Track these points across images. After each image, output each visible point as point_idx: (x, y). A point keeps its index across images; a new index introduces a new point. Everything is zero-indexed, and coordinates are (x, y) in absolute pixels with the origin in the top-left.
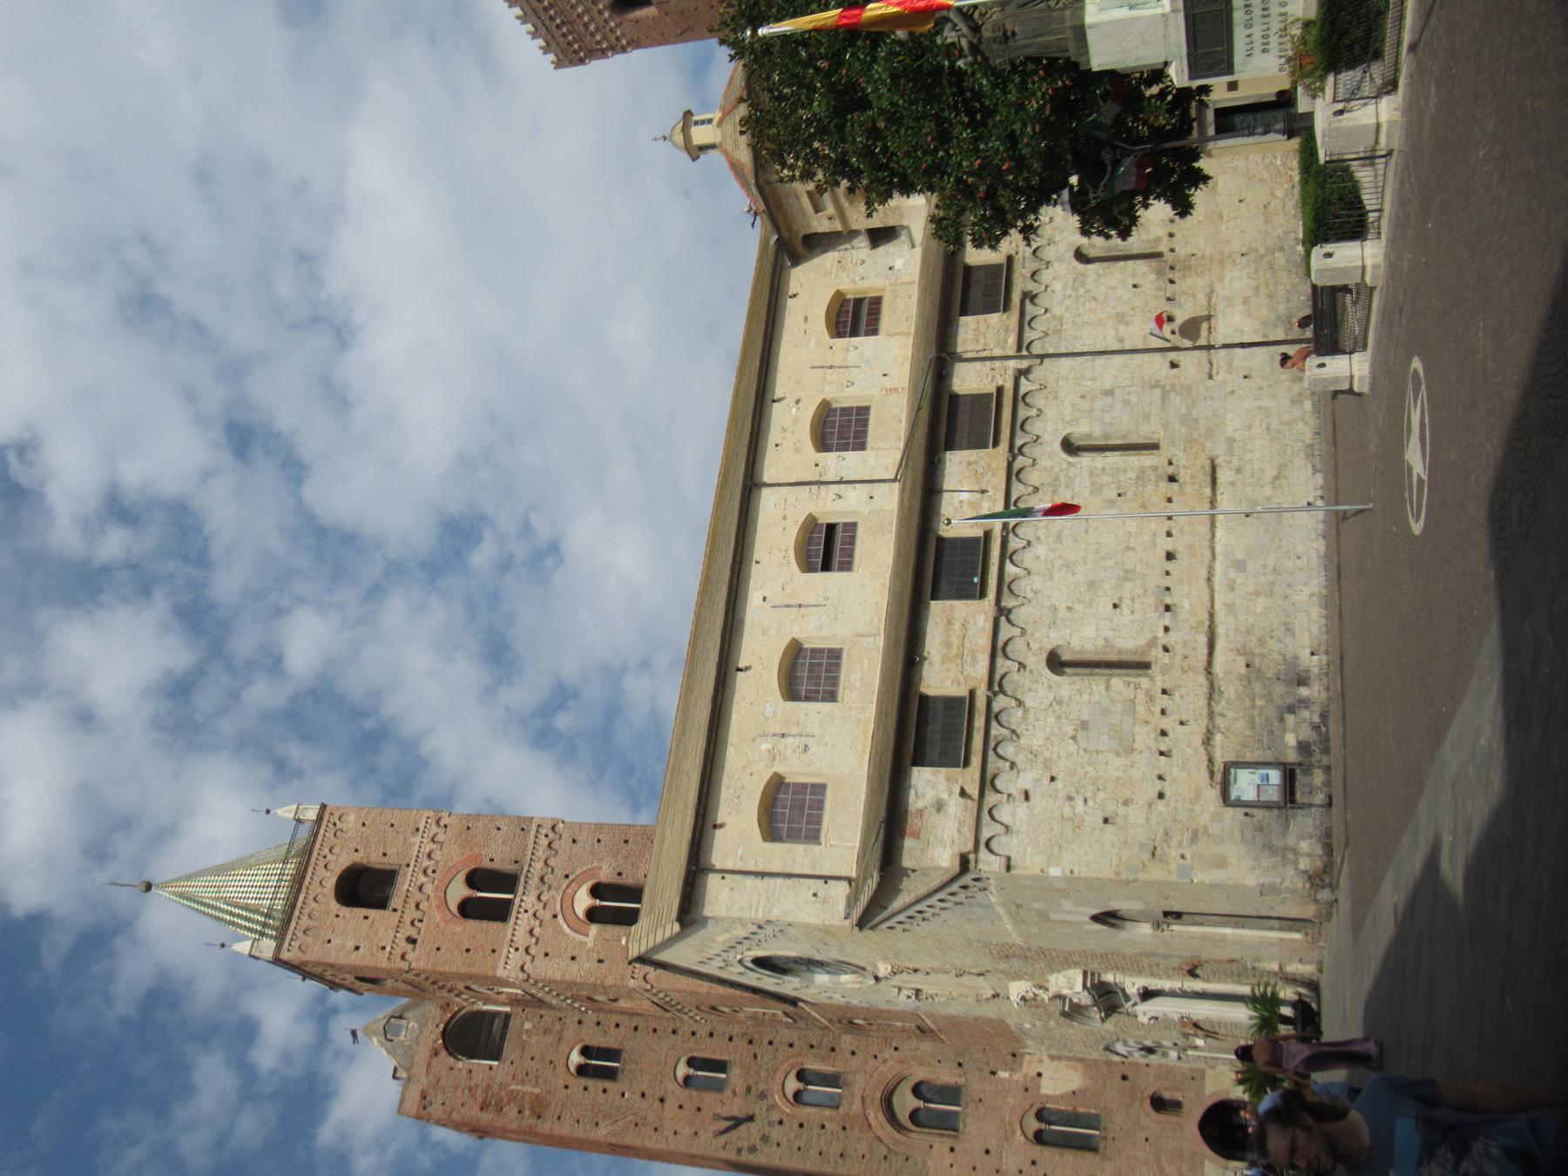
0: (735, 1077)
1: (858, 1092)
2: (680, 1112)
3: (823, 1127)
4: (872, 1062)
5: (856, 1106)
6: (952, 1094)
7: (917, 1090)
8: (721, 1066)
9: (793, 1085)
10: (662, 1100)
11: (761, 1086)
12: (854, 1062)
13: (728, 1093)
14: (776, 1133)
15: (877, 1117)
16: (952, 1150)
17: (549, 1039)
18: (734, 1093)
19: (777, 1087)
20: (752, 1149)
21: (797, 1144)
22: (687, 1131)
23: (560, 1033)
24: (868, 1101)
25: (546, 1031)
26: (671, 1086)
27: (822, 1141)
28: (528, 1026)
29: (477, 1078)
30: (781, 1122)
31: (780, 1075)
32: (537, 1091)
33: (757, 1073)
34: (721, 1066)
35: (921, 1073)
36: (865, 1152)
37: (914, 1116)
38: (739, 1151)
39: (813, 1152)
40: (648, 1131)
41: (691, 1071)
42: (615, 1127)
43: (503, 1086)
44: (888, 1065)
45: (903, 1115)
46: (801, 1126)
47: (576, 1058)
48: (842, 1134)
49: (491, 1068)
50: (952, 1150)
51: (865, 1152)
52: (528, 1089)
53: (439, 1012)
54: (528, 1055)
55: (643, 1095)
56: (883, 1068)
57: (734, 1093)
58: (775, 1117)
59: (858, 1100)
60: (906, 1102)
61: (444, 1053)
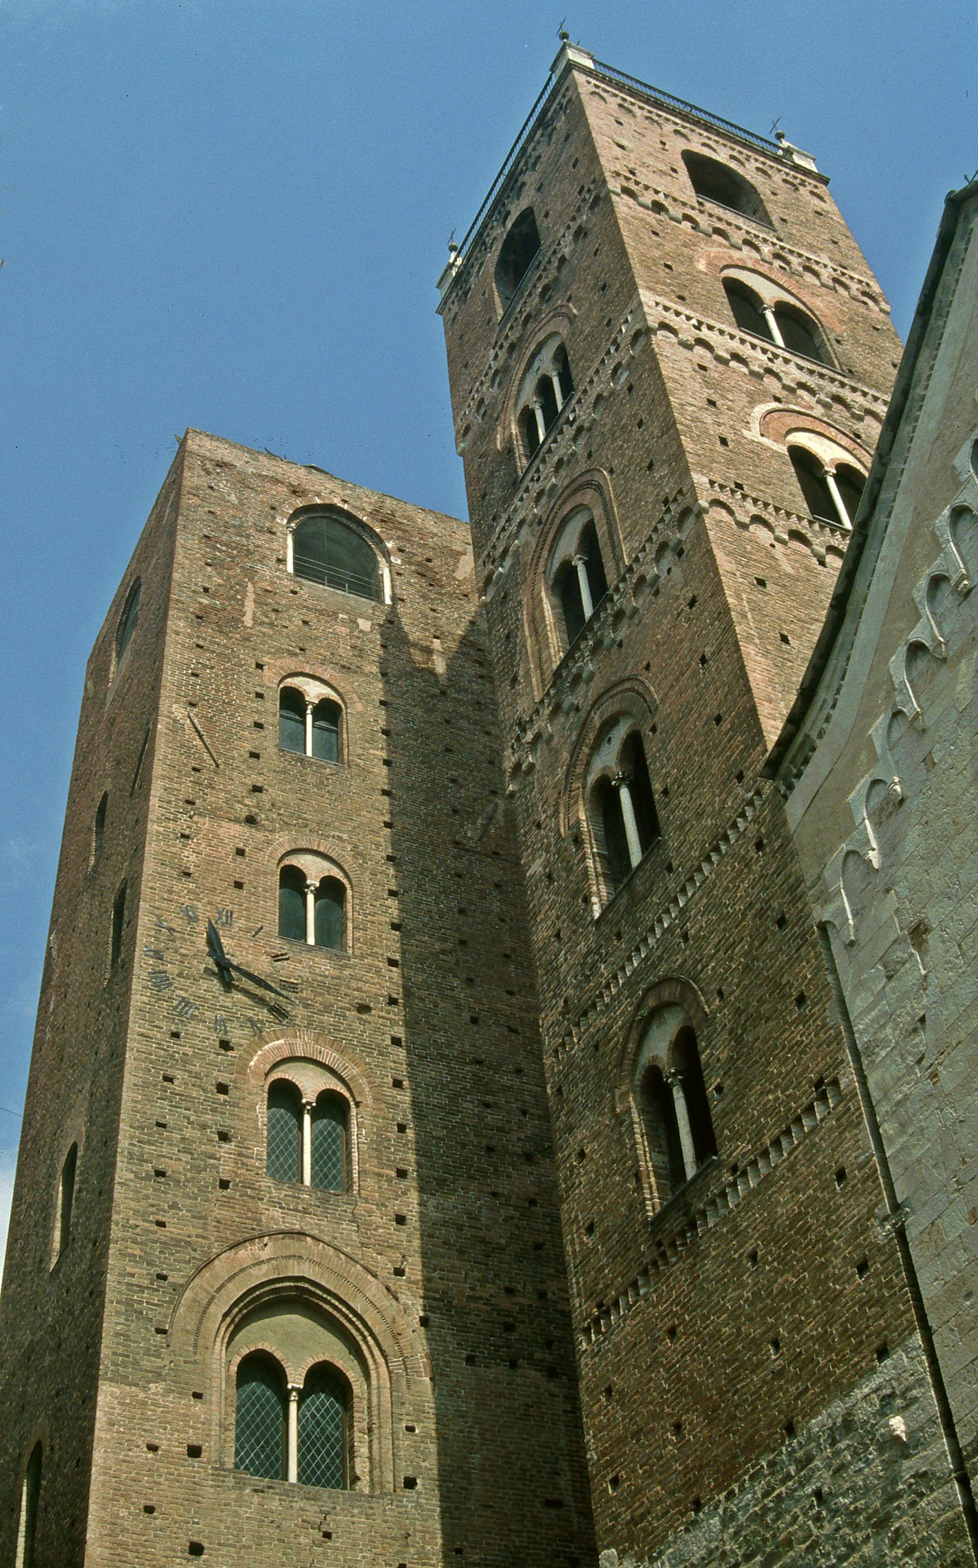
0: (308, 964)
1: (309, 1223)
2: (230, 849)
3: (224, 1137)
4: (384, 1264)
5: (275, 1217)
6: (330, 1466)
7: (325, 1378)
8: (331, 935)
9: (311, 1085)
10: (251, 820)
11: (299, 1012)
12: (381, 1220)
13: (279, 945)
14: (202, 1034)
15: (260, 1263)
16: (194, 1452)
17: (344, 651)
18: (277, 958)
19: (303, 1044)
20: (160, 981)
21: (179, 1074)
22: (190, 858)
23: (359, 671)
24: (294, 1246)
25: (359, 651)
26: (283, 841)
27: (189, 1133)
28: (365, 625)
29: (261, 539)
30: (225, 1045)
31: (329, 1056)
32: (248, 621)
33: (327, 1008)
34: (331, 935)
35: (372, 1390)
36: (172, 1230)
37: (261, 1369)
38: (158, 955)
39: (161, 1109)
40: (186, 788)
41: (313, 881)
42: (189, 732)
43: (251, 573)
44: (386, 1302)
45: (267, 1335)
46: (222, 1088)
47: (314, 692)
48: (207, 1177)
49: (281, 561)
50: (194, 1452)
51: (172, 1230)
52: (250, 607)
53: (369, 508)
54: (311, 617)
55: (257, 789)
56: (374, 1288)
57: (277, 958)
58: (237, 1035)
59: (296, 1224)
60: (298, 1345)
61: (300, 503)
